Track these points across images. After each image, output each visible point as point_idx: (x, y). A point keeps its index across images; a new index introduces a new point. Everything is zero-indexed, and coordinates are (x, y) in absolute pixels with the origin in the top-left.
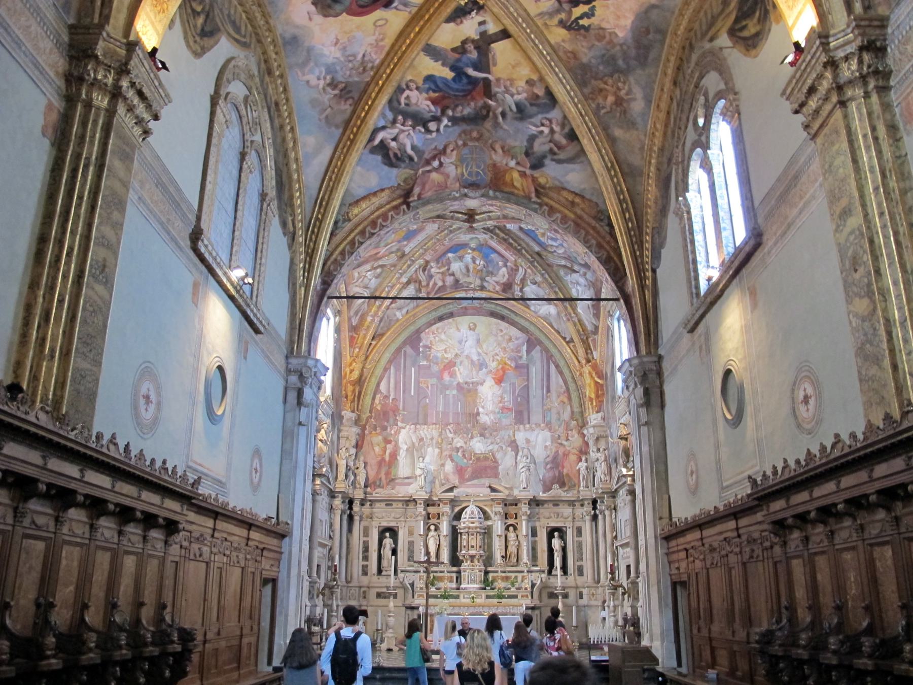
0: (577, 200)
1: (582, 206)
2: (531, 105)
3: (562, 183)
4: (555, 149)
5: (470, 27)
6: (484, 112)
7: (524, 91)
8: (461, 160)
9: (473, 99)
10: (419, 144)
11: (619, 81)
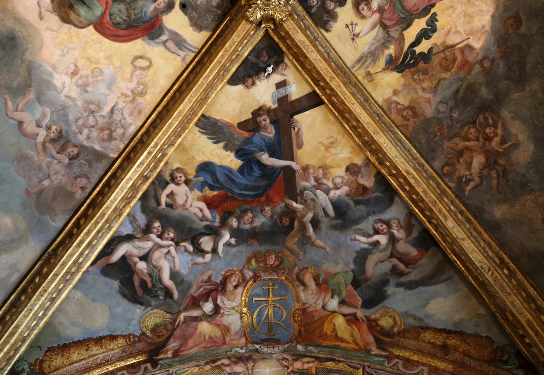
0: (453, 341)
1: (464, 347)
2: (357, 203)
3: (421, 320)
4: (401, 266)
5: (264, 92)
6: (286, 221)
7: (344, 184)
8: (251, 306)
9: (269, 201)
10: (184, 271)
11: (488, 125)
